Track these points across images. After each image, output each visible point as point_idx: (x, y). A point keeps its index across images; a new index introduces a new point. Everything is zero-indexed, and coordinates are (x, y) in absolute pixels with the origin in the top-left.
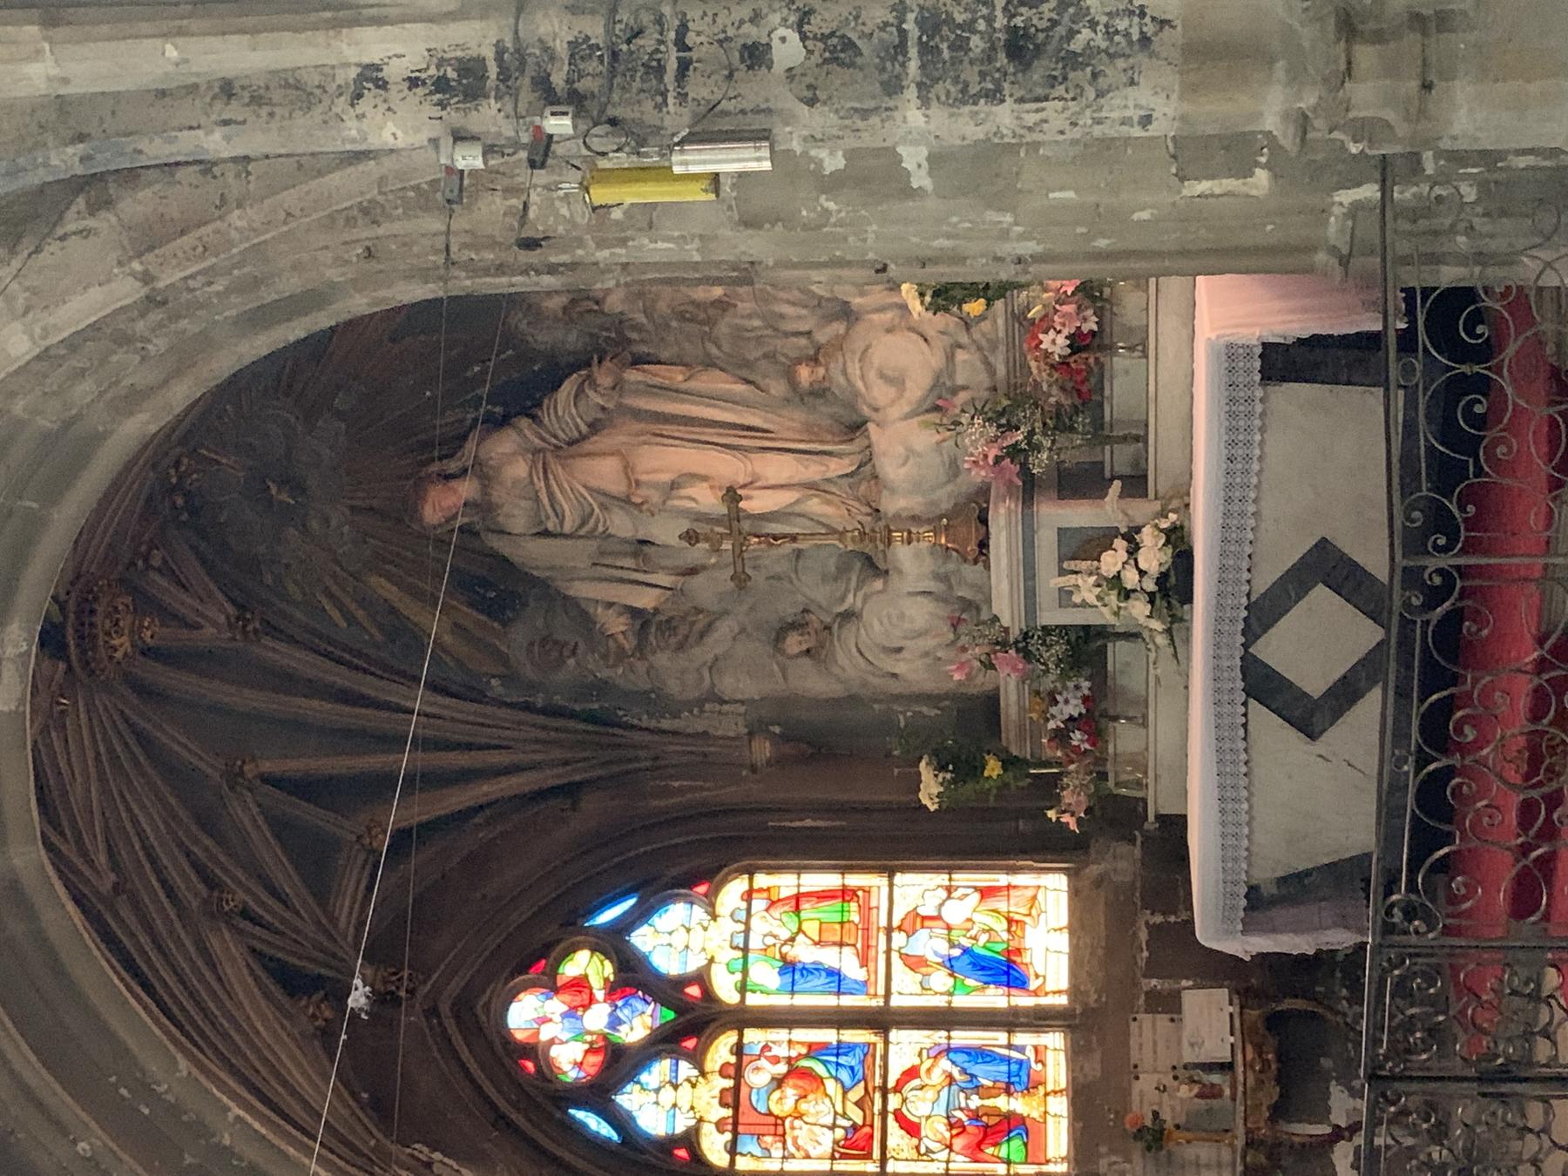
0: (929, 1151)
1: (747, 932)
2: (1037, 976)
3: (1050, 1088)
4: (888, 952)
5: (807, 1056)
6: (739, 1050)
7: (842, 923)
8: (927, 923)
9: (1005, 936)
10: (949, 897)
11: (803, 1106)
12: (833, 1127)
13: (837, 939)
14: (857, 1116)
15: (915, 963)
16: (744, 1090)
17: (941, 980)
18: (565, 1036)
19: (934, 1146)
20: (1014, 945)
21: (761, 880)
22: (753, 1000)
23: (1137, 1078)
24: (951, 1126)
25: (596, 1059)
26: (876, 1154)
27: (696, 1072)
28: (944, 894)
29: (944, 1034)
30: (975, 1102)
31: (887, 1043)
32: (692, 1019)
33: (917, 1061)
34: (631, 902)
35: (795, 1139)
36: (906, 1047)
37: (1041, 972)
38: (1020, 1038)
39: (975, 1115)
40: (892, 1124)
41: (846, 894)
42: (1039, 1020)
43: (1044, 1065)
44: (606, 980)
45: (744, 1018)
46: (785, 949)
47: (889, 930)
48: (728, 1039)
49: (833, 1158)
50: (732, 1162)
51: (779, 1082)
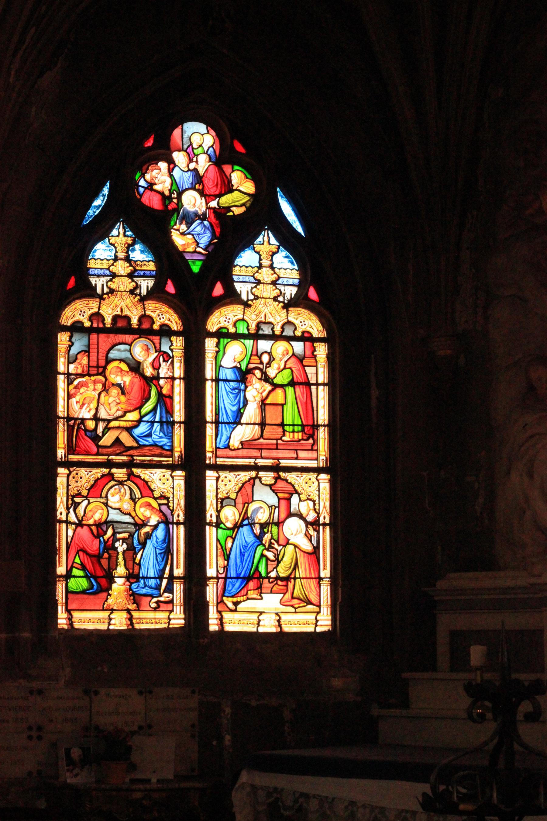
0: (76, 505)
1: (274, 337)
2: (236, 604)
3: (135, 614)
4: (257, 468)
5: (160, 395)
6: (166, 332)
7: (282, 425)
8: (283, 503)
9: (273, 574)
10: (307, 524)
11: (114, 391)
12: (96, 418)
13: (268, 421)
14: (107, 440)
15: (246, 493)
16: (128, 338)
17: (230, 515)
18: (176, 173)
19: (81, 510)
20: (266, 583)
21: (322, 350)
22: (210, 344)
23: (140, 693)
24: (98, 525)
25: (155, 203)
26: (74, 458)
27: (144, 292)
28: (311, 517)
30: (121, 547)
31: (172, 467)
32: (195, 291)
33: (157, 494)
34: (299, 229)
35: (85, 385)
36: (169, 484)
37: (240, 607)
38: (178, 587)
39: (110, 547)
40: (98, 472)
41: (310, 429)
42: (196, 605)
43: (155, 609)
44: (228, 209)
46: (258, 373)
47: (276, 469)
48: (175, 324)
49: (68, 419)
50: (65, 329)
51: (135, 368)
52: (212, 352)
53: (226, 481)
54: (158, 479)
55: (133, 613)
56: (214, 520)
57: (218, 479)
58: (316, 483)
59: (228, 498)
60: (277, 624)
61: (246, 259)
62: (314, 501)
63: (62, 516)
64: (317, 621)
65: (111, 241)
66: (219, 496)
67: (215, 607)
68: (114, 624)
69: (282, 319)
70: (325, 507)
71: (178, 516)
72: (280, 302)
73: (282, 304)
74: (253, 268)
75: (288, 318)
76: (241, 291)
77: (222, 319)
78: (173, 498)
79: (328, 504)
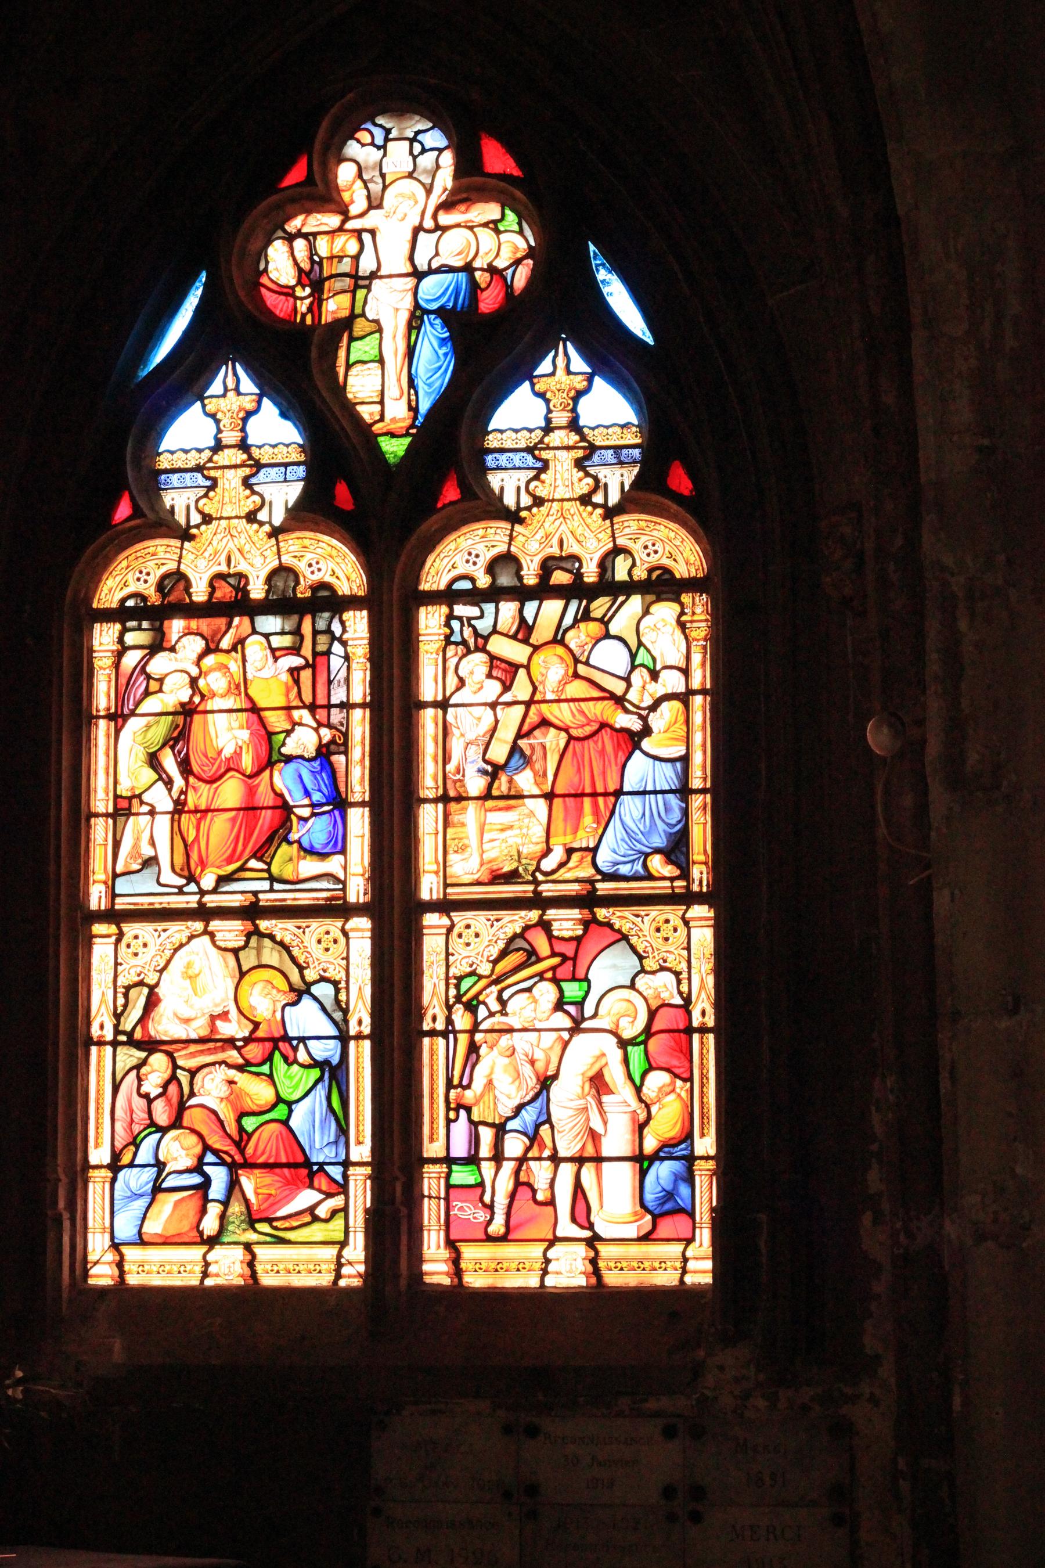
6: (327, 601)
29: (366, 1030)
45: (394, 606)
52: (436, 638)
53: (468, 935)
54: (314, 941)
55: (257, 1250)
56: (440, 1026)
57: (450, 930)
58: (682, 930)
59: (473, 973)
60: (590, 1268)
61: (517, 413)
62: (677, 974)
63: (104, 1032)
64: (685, 1260)
65: (207, 408)
66: (452, 971)
67: (442, 1234)
68: (217, 1275)
69: (601, 545)
70: (702, 987)
71: (360, 1022)
72: (596, 506)
73: (599, 511)
74: (531, 431)
75: (614, 541)
76: (502, 489)
77: (459, 560)
78: (347, 982)
79: (710, 981)
